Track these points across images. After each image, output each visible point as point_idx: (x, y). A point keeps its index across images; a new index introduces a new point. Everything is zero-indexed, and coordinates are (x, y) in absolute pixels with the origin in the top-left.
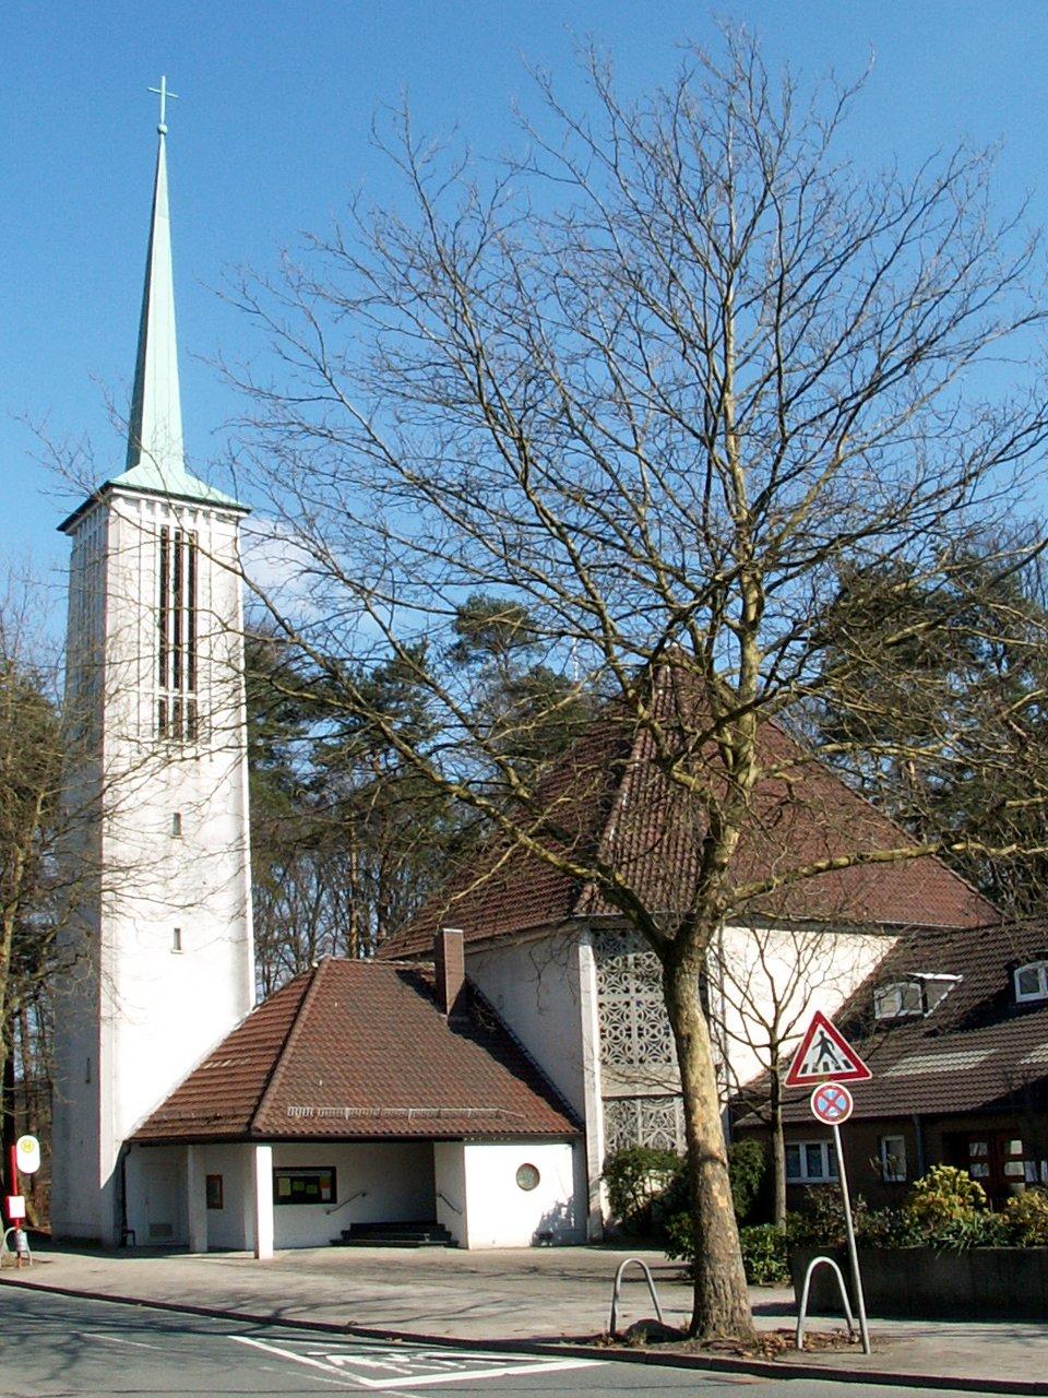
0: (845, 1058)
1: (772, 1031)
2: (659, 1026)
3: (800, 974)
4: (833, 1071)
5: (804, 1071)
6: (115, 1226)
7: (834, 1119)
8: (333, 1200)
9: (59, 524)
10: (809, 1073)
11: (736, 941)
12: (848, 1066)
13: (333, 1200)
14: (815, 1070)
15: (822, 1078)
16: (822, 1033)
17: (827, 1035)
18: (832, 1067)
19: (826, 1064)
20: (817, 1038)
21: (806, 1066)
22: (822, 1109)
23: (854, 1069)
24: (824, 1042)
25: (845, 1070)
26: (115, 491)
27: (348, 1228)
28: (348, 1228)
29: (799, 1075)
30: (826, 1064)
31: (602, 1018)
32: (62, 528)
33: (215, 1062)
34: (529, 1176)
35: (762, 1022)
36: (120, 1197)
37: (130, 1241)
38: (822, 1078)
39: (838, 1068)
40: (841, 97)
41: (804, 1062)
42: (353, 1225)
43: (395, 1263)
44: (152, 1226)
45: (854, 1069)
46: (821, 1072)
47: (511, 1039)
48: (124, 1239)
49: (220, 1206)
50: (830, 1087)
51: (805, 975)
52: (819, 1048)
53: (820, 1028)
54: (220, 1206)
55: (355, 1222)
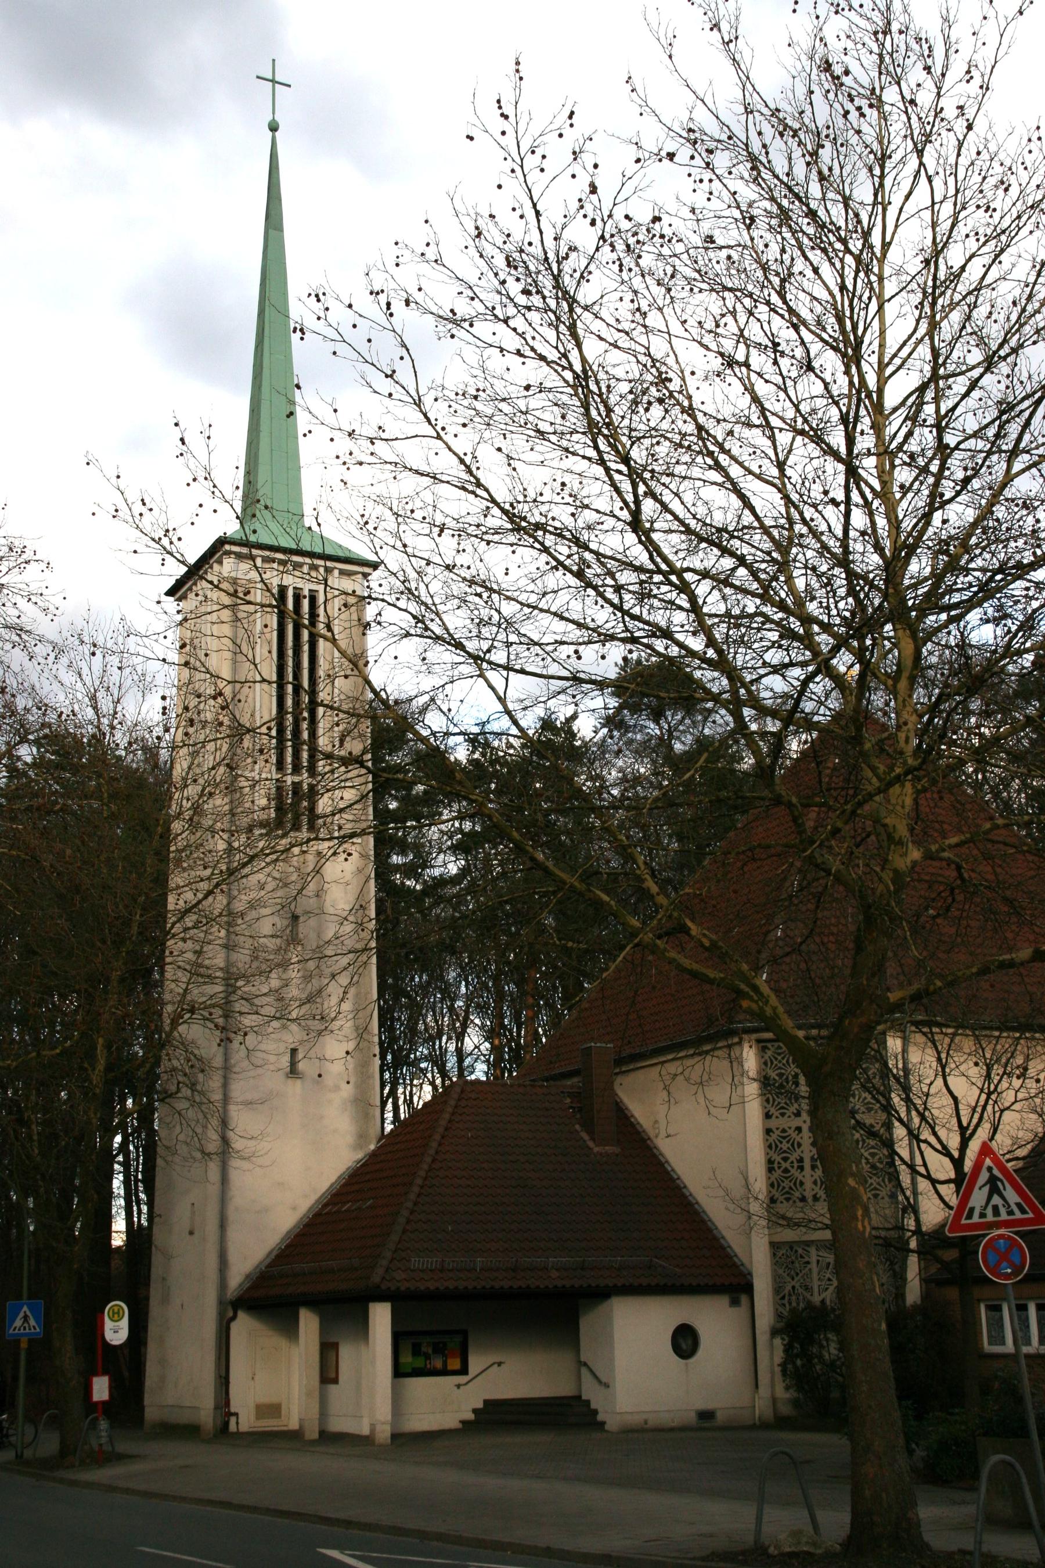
0: (1019, 1200)
1: (958, 1164)
2: (779, 1172)
3: (989, 1094)
4: (1004, 1216)
5: (970, 1216)
6: (216, 1408)
7: (1007, 1276)
8: (464, 1371)
9: (171, 582)
10: (976, 1219)
11: (909, 1053)
12: (1023, 1211)
13: (464, 1371)
14: (982, 1215)
15: (991, 1226)
16: (990, 1169)
17: (996, 1172)
18: (1003, 1211)
19: (996, 1209)
20: (984, 1176)
21: (972, 1210)
22: (992, 1264)
23: (1031, 1215)
24: (992, 1180)
25: (1018, 1215)
26: (227, 547)
27: (480, 1405)
28: (480, 1405)
29: (963, 1222)
30: (996, 1209)
31: (770, 1147)
32: (170, 593)
33: (335, 1204)
34: (685, 1342)
35: (947, 1153)
36: (223, 1374)
37: (233, 1427)
38: (991, 1226)
39: (1010, 1213)
40: (1003, 25)
41: (970, 1205)
42: (486, 1402)
43: (1028, 1327)
44: (258, 1407)
45: (1031, 1215)
46: (990, 1217)
47: (668, 1173)
48: (226, 1424)
49: (335, 1381)
50: (1001, 1236)
51: (994, 1097)
52: (987, 1189)
53: (988, 1162)
54: (335, 1381)
55: (488, 1397)
